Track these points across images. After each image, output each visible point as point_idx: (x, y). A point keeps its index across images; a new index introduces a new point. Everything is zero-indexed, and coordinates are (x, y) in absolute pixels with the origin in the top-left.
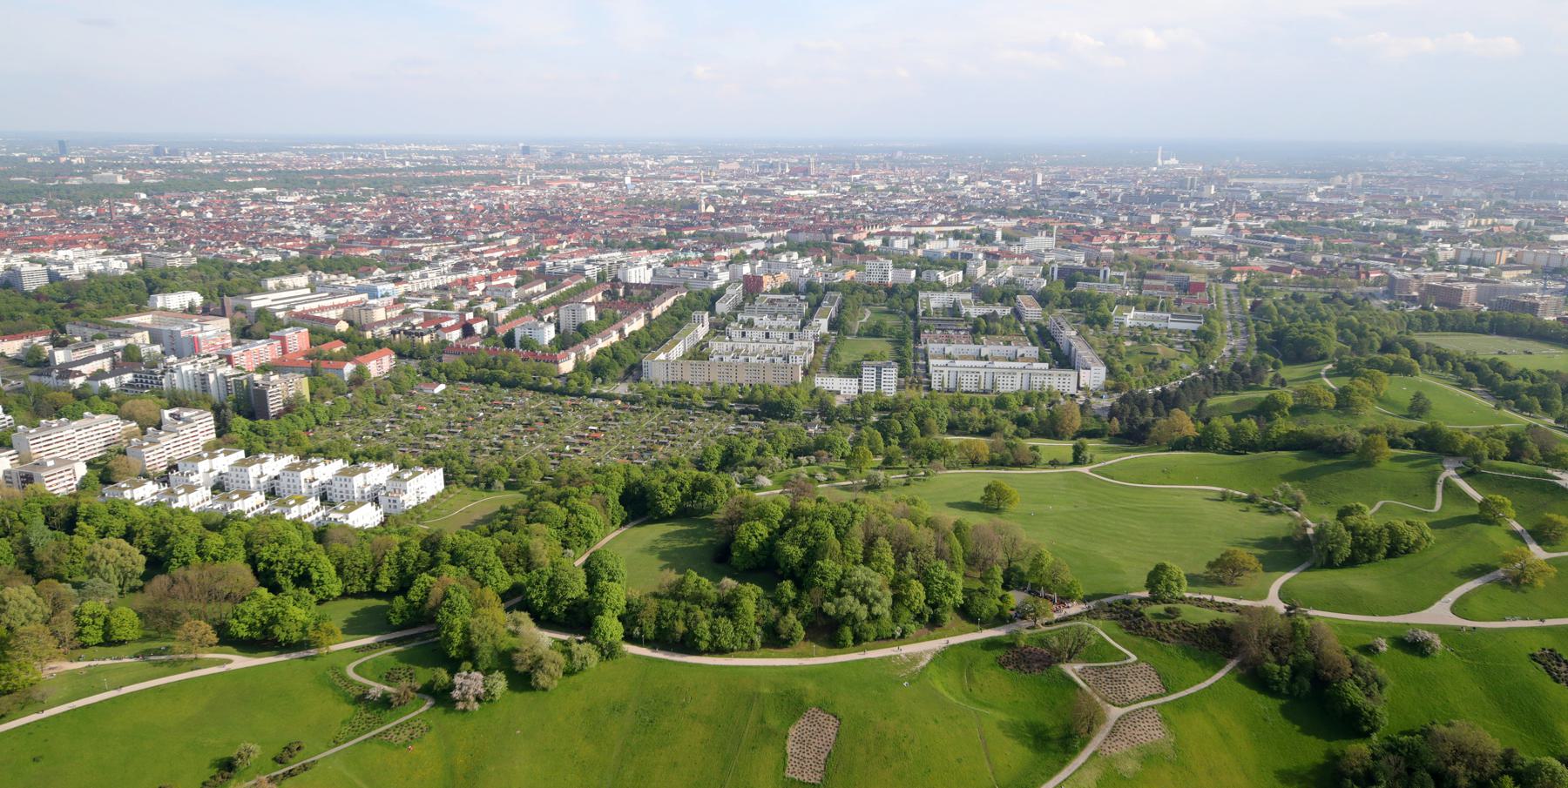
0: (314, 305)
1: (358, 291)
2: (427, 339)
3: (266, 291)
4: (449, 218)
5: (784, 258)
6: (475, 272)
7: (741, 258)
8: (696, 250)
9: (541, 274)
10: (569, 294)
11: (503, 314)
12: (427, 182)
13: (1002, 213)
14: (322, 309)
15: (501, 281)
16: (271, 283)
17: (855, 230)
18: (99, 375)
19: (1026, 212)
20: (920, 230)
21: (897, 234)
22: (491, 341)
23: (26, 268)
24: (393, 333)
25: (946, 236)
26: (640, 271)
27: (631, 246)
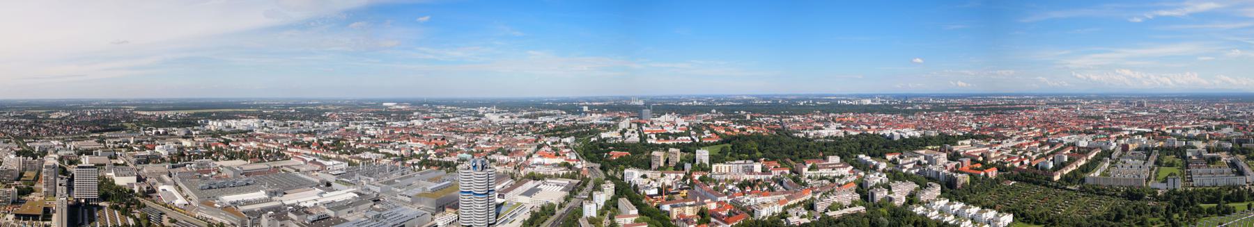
0: (972, 151)
1: (986, 146)
2: (1008, 165)
3: (958, 145)
4: (1016, 122)
5: (1136, 138)
6: (1024, 141)
7: (1119, 138)
8: (1104, 135)
9: (1048, 143)
10: (1058, 150)
11: (1034, 157)
12: (1010, 109)
13: (1215, 119)
14: (974, 152)
15: (1034, 145)
16: (960, 142)
17: (1162, 127)
18: (910, 169)
19: (1222, 119)
20: (1186, 127)
21: (1178, 129)
22: (1030, 167)
23: (895, 134)
24: (997, 162)
25: (1195, 129)
26: (1083, 143)
27: (1080, 133)
